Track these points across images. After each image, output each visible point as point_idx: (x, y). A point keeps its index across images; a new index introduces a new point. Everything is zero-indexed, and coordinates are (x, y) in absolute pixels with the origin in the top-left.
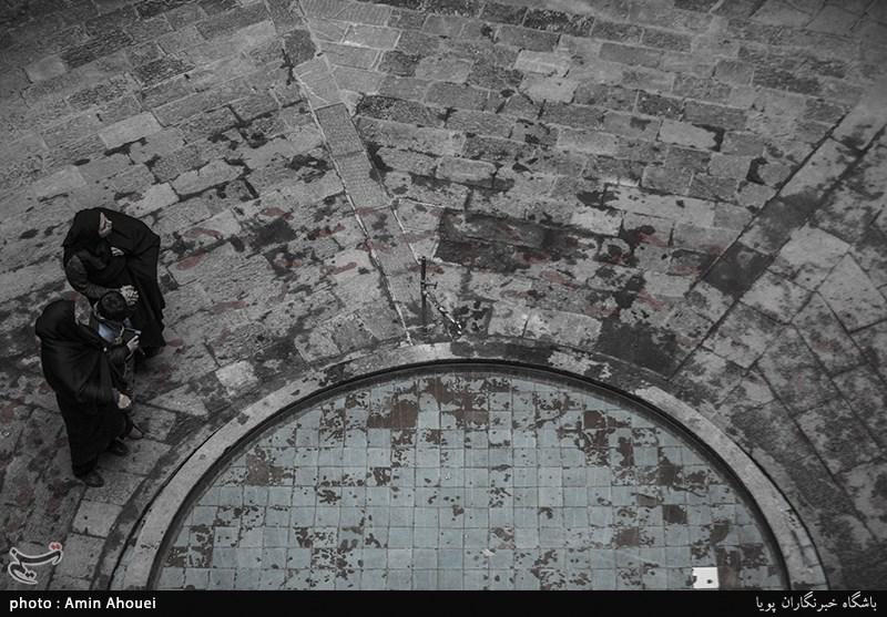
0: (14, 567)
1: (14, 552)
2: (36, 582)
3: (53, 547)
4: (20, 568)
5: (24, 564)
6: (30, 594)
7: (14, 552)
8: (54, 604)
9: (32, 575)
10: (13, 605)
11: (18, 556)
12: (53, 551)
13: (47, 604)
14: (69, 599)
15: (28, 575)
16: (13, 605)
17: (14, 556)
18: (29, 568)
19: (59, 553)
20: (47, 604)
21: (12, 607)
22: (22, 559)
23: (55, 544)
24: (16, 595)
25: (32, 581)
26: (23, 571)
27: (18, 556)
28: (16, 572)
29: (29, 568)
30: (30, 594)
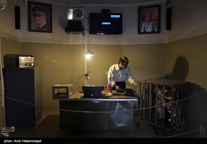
0: (3, 132)
3: (12, 128)
5: (5, 132)
7: (3, 129)
8: (13, 141)
9: (7, 134)
10: (5, 141)
11: (4, 130)
13: (11, 141)
14: (15, 140)
15: (6, 134)
16: (5, 141)
18: (7, 133)
19: (13, 129)
20: (11, 141)
21: (4, 142)
22: (5, 130)
23: (13, 127)
25: (8, 136)
26: (5, 133)
27: (4, 130)
28: (4, 133)
29: (7, 133)
30: (8, 139)
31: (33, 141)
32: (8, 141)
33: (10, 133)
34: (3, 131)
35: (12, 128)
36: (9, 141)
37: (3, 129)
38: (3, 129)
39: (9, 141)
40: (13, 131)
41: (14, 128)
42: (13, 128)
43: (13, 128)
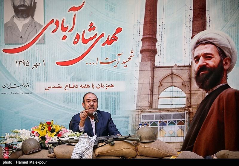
1: (3, 149)
4: (5, 153)
6: (7, 160)
7: (3, 149)
8: (13, 163)
9: (8, 155)
13: (11, 163)
15: (7, 155)
16: (4, 163)
17: (4, 150)
20: (11, 163)
21: (3, 163)
24: (4, 160)
27: (5, 150)
28: (4, 154)
30: (7, 160)
32: (7, 163)
34: (3, 151)
36: (8, 163)
39: (8, 163)
43: (15, 148)
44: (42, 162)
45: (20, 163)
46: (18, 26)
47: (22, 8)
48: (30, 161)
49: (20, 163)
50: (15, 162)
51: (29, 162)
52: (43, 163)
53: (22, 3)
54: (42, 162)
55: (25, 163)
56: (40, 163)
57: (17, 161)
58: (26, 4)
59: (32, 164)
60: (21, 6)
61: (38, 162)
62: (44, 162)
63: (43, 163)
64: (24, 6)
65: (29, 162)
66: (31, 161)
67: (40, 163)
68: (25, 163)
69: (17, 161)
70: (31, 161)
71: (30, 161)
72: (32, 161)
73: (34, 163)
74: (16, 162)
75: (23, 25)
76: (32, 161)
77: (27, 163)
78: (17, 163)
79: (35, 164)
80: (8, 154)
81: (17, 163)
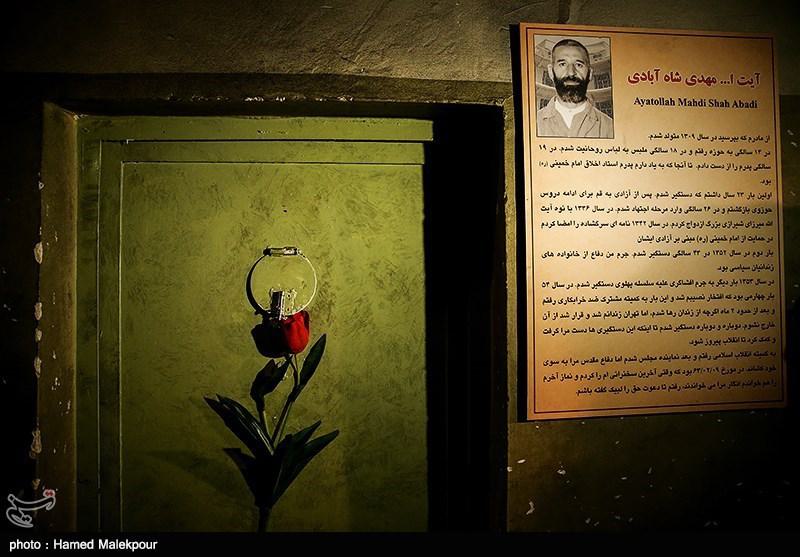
0: (11, 512)
1: (11, 498)
2: (32, 526)
7: (11, 498)
8: (43, 546)
9: (28, 519)
10: (14, 545)
11: (15, 502)
12: (47, 497)
13: (37, 545)
15: (24, 519)
16: (14, 545)
17: (12, 502)
18: (26, 513)
19: (51, 500)
20: (37, 545)
21: (11, 548)
23: (49, 491)
25: (28, 524)
26: (20, 516)
27: (15, 502)
28: (13, 516)
29: (26, 513)
30: (25, 535)
31: (126, 545)
32: (23, 546)
33: (41, 518)
35: (44, 494)
36: (27, 545)
37: (11, 498)
38: (11, 498)
39: (27, 545)
40: (49, 507)
41: (51, 494)
42: (50, 493)
43: (49, 496)
44: (139, 545)
45: (66, 545)
46: (564, 117)
47: (571, 83)
48: (100, 541)
49: (66, 545)
50: (52, 544)
51: (96, 544)
52: (142, 545)
53: (571, 74)
54: (139, 545)
55: (83, 545)
56: (135, 545)
57: (58, 541)
58: (578, 76)
59: (107, 552)
60: (568, 78)
61: (128, 545)
62: (146, 545)
63: (142, 545)
64: (574, 79)
65: (96, 544)
66: (103, 542)
67: (135, 545)
68: (83, 545)
69: (58, 541)
70: (103, 542)
71: (100, 541)
72: (107, 541)
73: (113, 546)
74: (55, 544)
75: (574, 116)
76: (107, 541)
77: (90, 545)
78: (58, 546)
79: (118, 552)
80: (25, 516)
81: (58, 546)
